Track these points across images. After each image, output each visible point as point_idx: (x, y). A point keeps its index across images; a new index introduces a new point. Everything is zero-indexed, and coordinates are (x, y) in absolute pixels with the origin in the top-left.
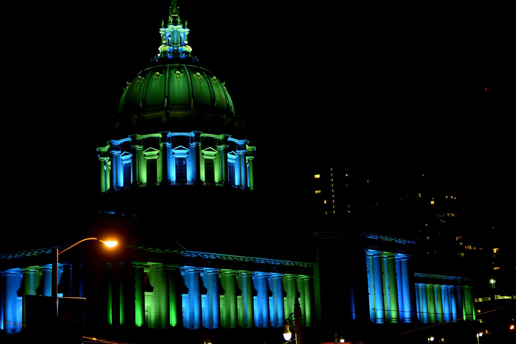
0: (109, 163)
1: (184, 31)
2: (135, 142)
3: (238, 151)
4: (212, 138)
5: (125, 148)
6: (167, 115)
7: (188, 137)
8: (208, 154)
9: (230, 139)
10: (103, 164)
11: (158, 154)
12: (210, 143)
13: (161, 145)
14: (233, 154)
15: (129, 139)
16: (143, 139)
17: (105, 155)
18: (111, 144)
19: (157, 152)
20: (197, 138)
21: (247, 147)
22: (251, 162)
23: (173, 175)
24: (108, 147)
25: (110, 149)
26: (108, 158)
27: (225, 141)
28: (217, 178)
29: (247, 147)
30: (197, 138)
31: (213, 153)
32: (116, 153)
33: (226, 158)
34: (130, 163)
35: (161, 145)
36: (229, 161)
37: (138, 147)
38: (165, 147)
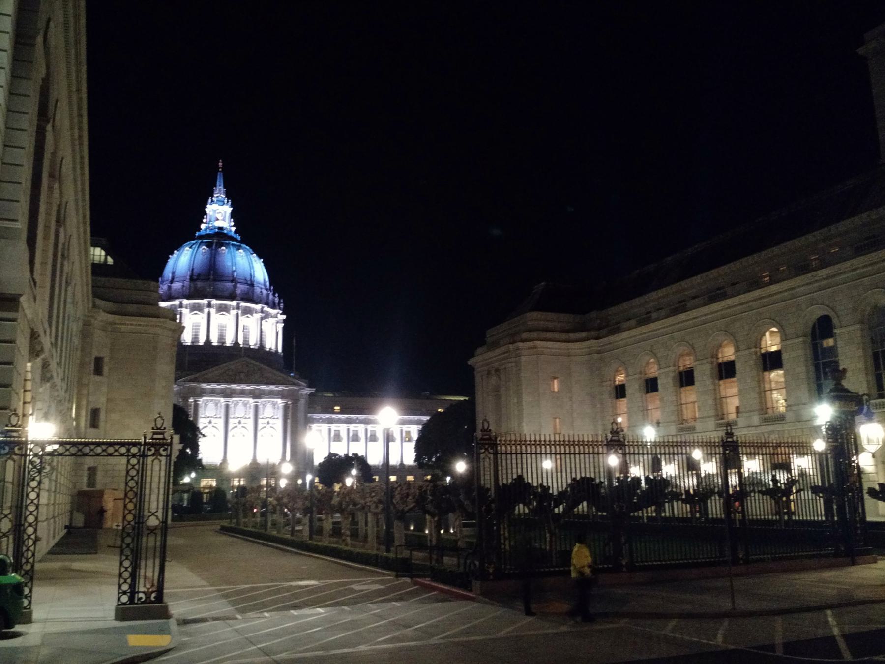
1: (228, 209)
12: (247, 312)
20: (238, 308)
27: (262, 311)
30: (238, 308)
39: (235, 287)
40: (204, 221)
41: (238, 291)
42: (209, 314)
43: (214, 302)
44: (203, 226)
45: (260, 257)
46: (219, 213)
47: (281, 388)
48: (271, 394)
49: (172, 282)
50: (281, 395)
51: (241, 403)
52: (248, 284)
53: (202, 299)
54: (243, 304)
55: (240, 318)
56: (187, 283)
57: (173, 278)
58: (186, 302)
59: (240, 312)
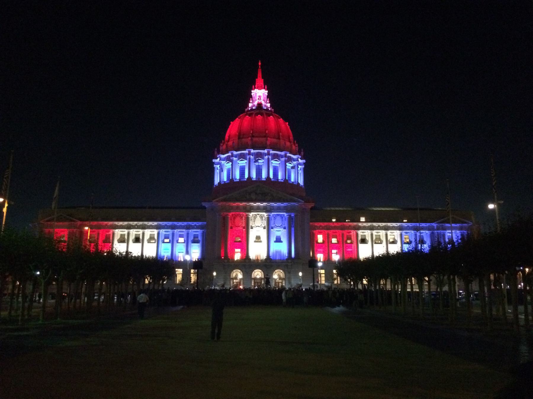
0: (219, 168)
5: (228, 159)
6: (252, 140)
8: (275, 163)
9: (288, 155)
10: (216, 169)
12: (275, 157)
13: (248, 157)
15: (230, 154)
17: (218, 164)
19: (246, 161)
20: (268, 154)
21: (299, 159)
22: (302, 169)
23: (254, 176)
24: (219, 159)
28: (280, 177)
29: (299, 159)
32: (223, 162)
33: (286, 165)
35: (248, 157)
36: (287, 167)
37: (235, 159)
38: (250, 158)
39: (267, 140)
40: (251, 101)
41: (268, 143)
43: (252, 151)
44: (250, 105)
45: (286, 120)
46: (259, 95)
47: (285, 204)
48: (279, 209)
49: (228, 141)
50: (286, 209)
51: (258, 216)
52: (277, 139)
54: (272, 152)
56: (236, 141)
57: (229, 139)
58: (235, 153)
59: (270, 157)
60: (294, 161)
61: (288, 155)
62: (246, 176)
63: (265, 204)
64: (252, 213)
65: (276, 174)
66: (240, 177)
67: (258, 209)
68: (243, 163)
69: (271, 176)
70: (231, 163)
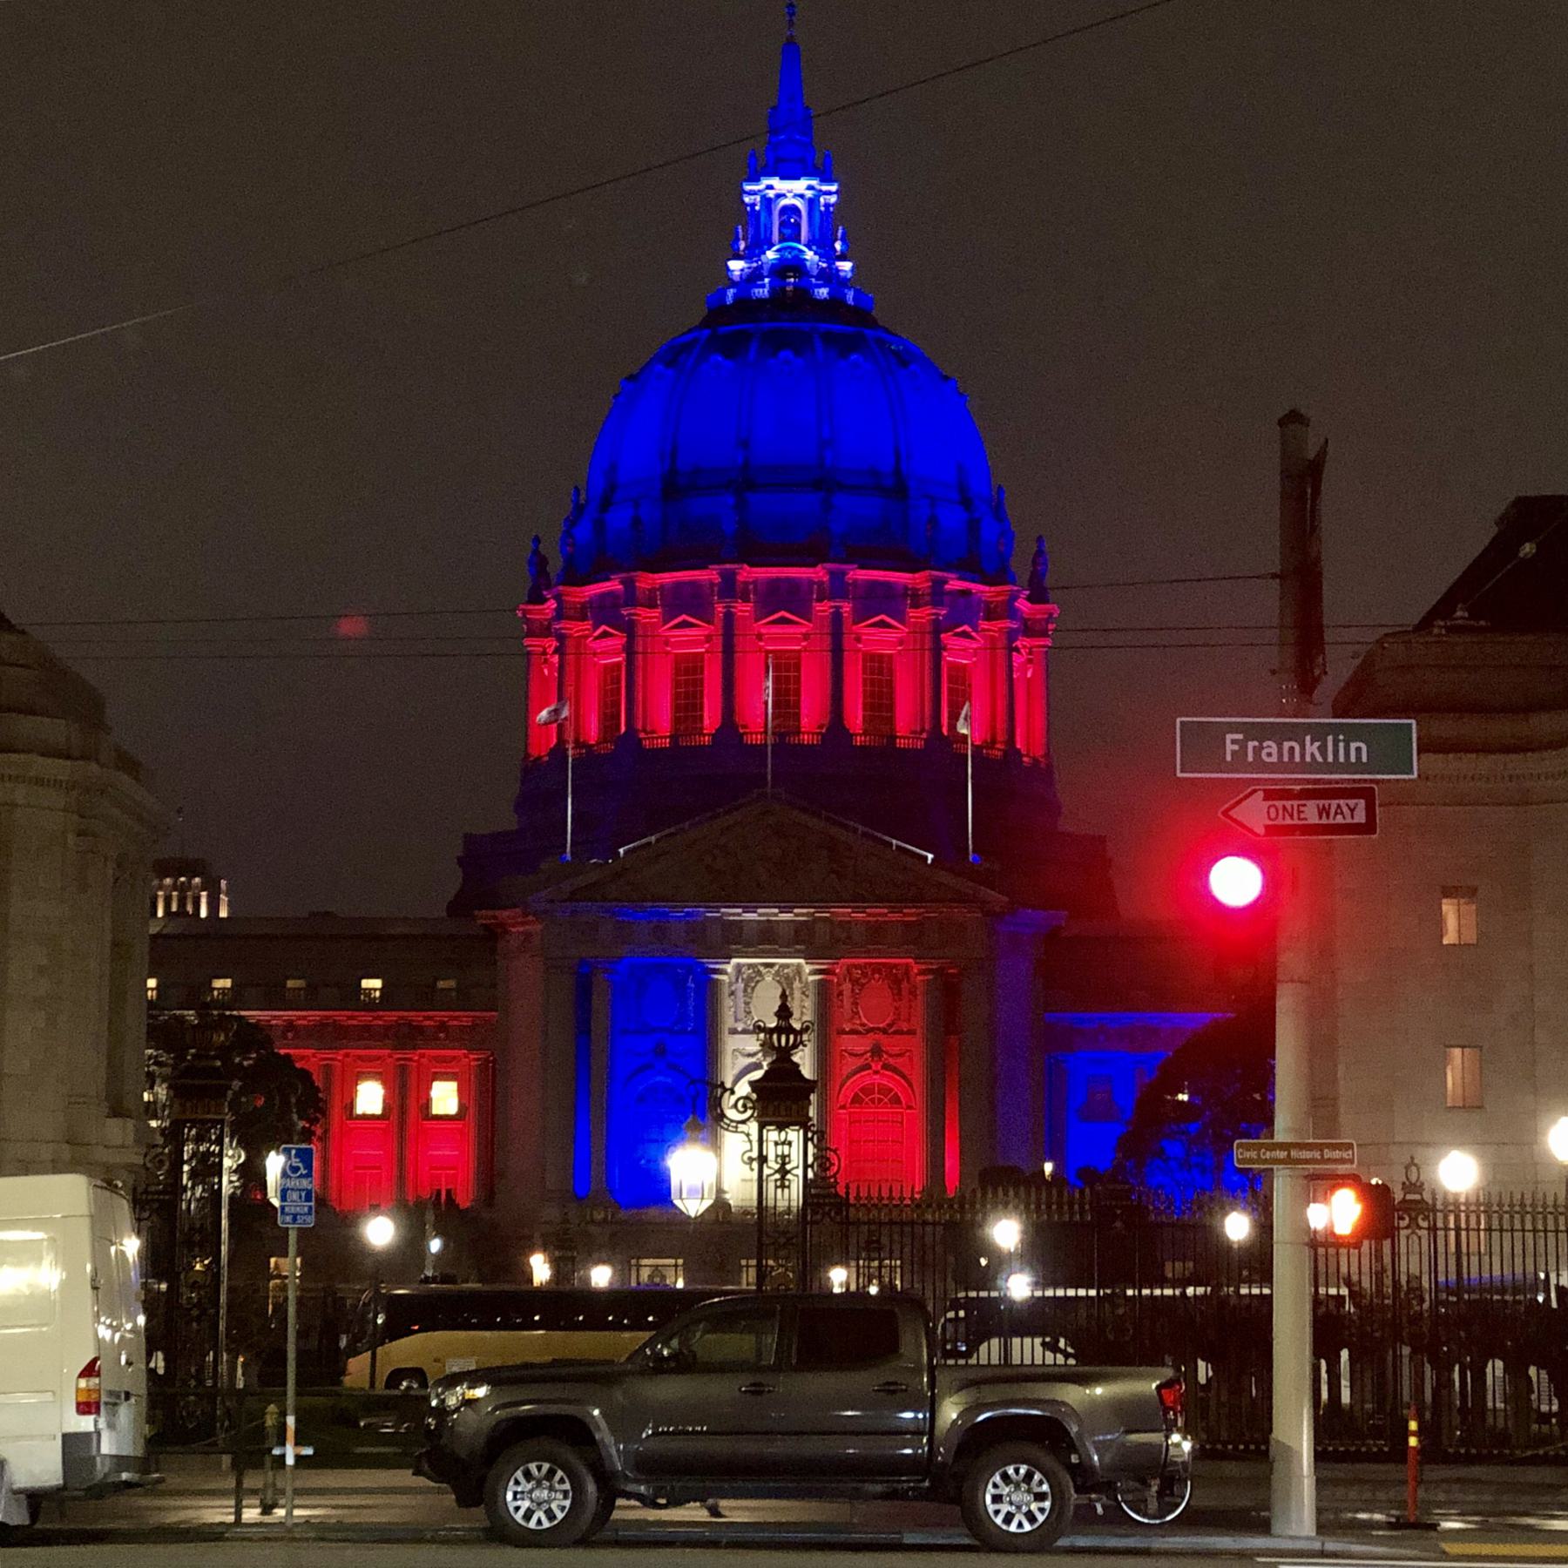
2: (630, 597)
3: (984, 625)
4: (887, 586)
7: (811, 582)
11: (708, 639)
13: (720, 609)
14: (965, 635)
16: (662, 586)
18: (558, 598)
20: (838, 588)
25: (560, 615)
26: (555, 644)
31: (892, 636)
32: (575, 629)
33: (938, 650)
34: (618, 664)
35: (720, 609)
42: (729, 616)
43: (748, 574)
53: (703, 567)
55: (851, 629)
59: (846, 608)
60: (989, 617)
61: (954, 584)
62: (710, 719)
63: (800, 914)
64: (734, 961)
65: (880, 704)
66: (677, 721)
67: (767, 940)
68: (691, 638)
69: (856, 719)
70: (619, 640)
